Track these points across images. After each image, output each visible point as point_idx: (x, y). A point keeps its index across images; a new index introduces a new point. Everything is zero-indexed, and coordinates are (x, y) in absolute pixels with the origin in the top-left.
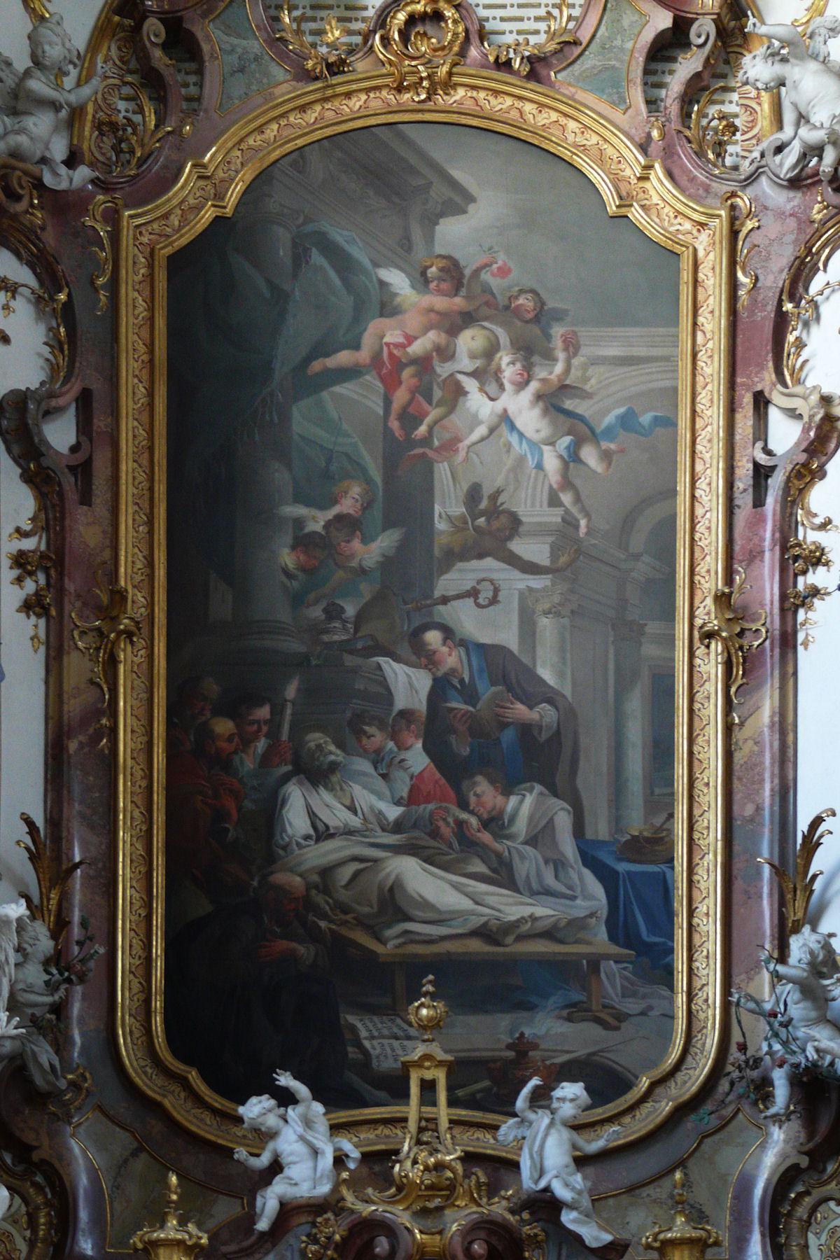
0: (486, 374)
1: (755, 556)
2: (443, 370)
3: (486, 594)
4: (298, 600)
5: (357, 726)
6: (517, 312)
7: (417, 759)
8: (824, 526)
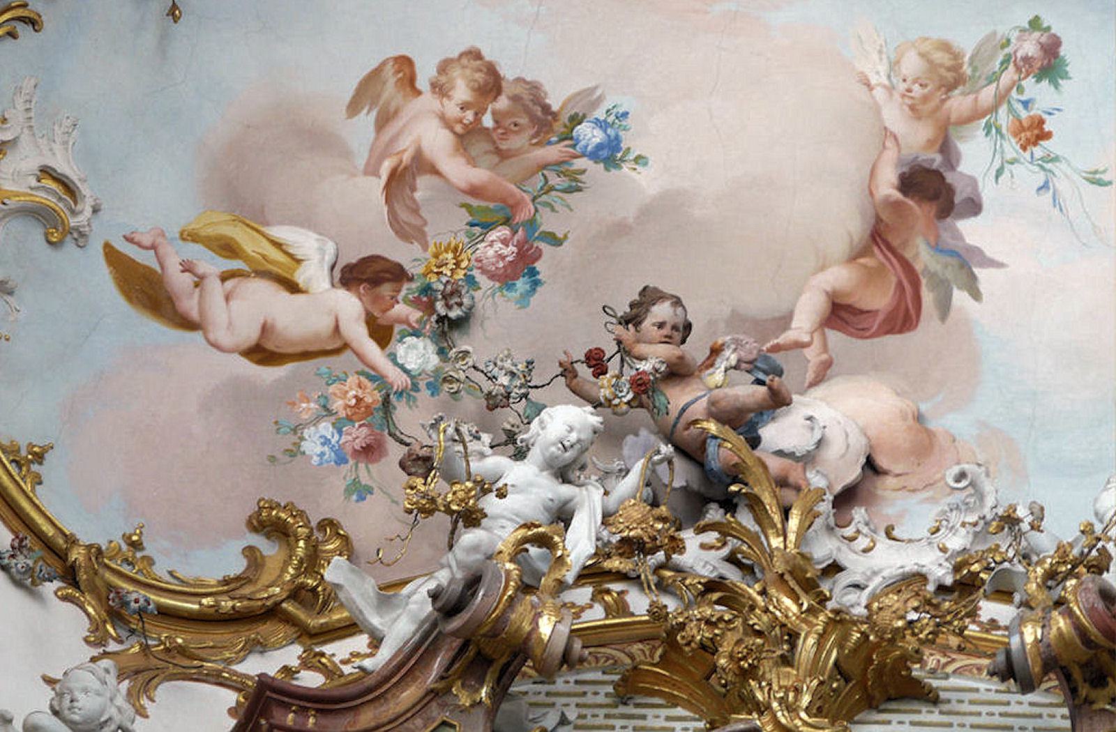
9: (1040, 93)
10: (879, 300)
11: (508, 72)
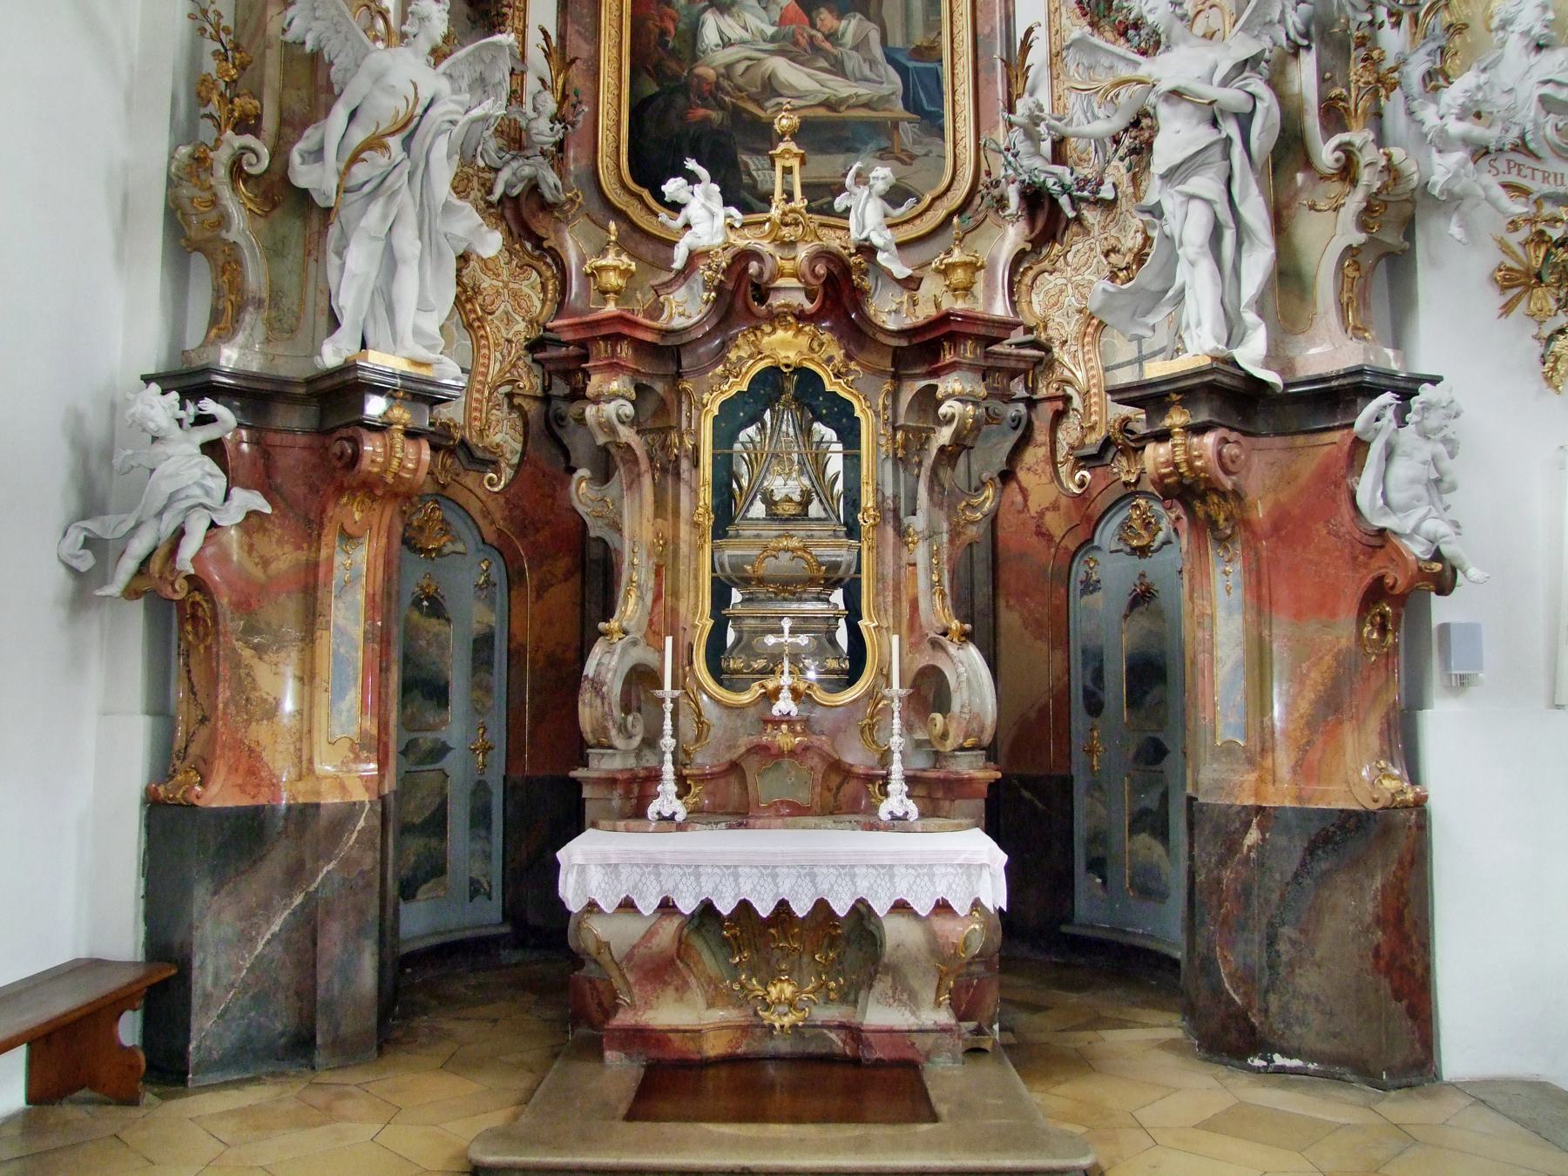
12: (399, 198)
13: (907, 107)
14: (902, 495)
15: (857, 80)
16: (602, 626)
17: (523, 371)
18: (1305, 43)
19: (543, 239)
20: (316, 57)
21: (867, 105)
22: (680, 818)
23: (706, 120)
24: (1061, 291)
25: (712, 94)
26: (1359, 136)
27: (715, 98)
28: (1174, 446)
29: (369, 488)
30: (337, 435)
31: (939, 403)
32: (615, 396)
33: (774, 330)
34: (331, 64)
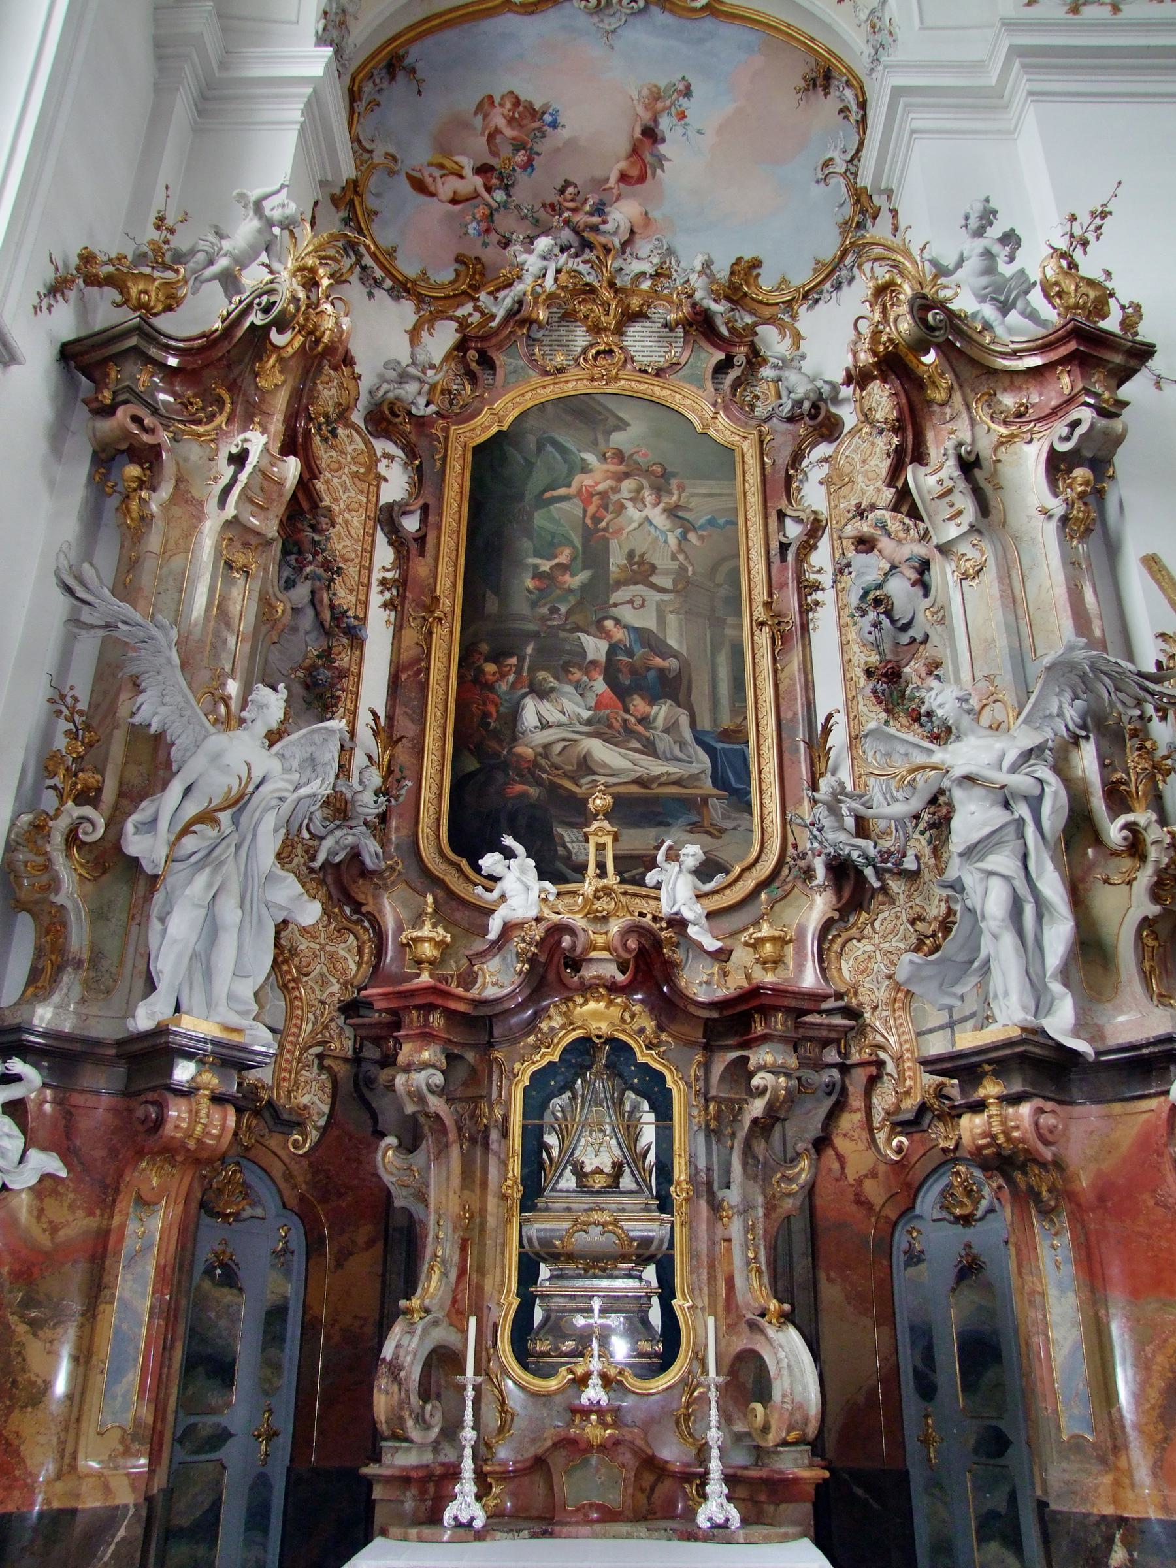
0: (637, 499)
1: (783, 585)
2: (614, 497)
3: (638, 602)
4: (534, 604)
5: (566, 668)
6: (653, 473)
7: (600, 685)
8: (819, 571)
9: (683, 101)
10: (635, 172)
11: (522, 98)
12: (224, 869)
13: (715, 784)
14: (716, 1167)
15: (668, 760)
16: (403, 1303)
17: (334, 1033)
18: (1084, 733)
19: (361, 904)
20: (159, 737)
21: (678, 783)
22: (478, 1524)
23: (525, 795)
24: (870, 958)
25: (530, 771)
26: (1143, 816)
27: (533, 775)
28: (990, 1117)
29: (170, 1152)
30: (143, 1098)
31: (751, 1075)
32: (425, 1066)
33: (586, 1002)
34: (173, 744)
